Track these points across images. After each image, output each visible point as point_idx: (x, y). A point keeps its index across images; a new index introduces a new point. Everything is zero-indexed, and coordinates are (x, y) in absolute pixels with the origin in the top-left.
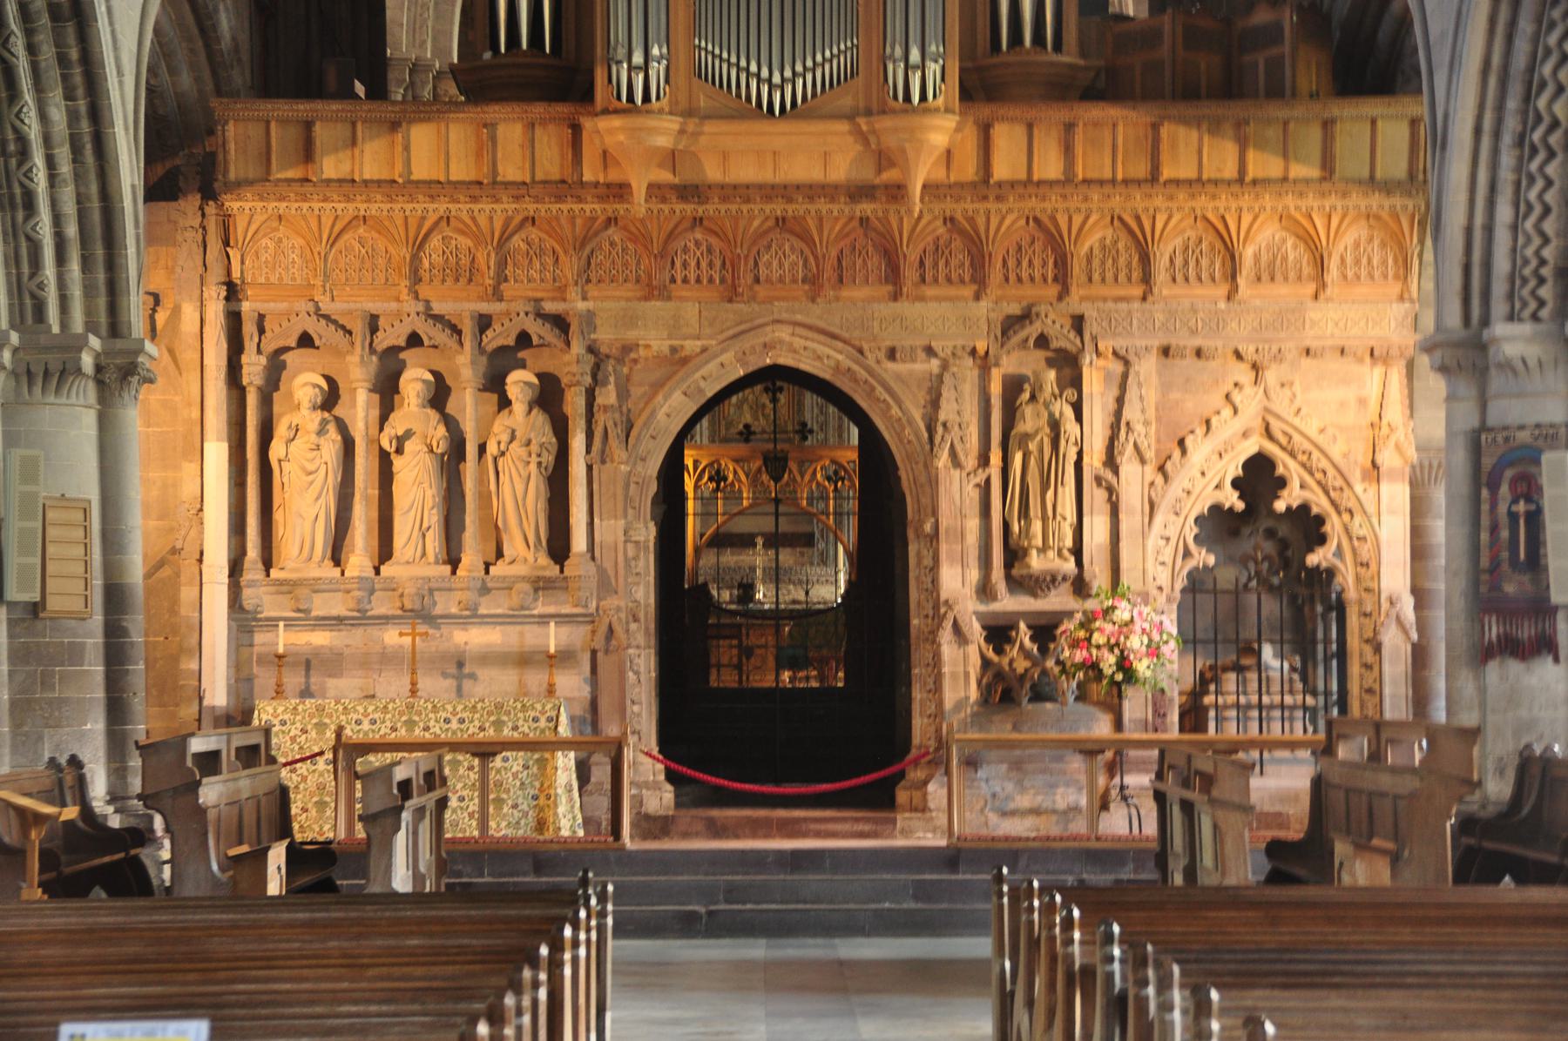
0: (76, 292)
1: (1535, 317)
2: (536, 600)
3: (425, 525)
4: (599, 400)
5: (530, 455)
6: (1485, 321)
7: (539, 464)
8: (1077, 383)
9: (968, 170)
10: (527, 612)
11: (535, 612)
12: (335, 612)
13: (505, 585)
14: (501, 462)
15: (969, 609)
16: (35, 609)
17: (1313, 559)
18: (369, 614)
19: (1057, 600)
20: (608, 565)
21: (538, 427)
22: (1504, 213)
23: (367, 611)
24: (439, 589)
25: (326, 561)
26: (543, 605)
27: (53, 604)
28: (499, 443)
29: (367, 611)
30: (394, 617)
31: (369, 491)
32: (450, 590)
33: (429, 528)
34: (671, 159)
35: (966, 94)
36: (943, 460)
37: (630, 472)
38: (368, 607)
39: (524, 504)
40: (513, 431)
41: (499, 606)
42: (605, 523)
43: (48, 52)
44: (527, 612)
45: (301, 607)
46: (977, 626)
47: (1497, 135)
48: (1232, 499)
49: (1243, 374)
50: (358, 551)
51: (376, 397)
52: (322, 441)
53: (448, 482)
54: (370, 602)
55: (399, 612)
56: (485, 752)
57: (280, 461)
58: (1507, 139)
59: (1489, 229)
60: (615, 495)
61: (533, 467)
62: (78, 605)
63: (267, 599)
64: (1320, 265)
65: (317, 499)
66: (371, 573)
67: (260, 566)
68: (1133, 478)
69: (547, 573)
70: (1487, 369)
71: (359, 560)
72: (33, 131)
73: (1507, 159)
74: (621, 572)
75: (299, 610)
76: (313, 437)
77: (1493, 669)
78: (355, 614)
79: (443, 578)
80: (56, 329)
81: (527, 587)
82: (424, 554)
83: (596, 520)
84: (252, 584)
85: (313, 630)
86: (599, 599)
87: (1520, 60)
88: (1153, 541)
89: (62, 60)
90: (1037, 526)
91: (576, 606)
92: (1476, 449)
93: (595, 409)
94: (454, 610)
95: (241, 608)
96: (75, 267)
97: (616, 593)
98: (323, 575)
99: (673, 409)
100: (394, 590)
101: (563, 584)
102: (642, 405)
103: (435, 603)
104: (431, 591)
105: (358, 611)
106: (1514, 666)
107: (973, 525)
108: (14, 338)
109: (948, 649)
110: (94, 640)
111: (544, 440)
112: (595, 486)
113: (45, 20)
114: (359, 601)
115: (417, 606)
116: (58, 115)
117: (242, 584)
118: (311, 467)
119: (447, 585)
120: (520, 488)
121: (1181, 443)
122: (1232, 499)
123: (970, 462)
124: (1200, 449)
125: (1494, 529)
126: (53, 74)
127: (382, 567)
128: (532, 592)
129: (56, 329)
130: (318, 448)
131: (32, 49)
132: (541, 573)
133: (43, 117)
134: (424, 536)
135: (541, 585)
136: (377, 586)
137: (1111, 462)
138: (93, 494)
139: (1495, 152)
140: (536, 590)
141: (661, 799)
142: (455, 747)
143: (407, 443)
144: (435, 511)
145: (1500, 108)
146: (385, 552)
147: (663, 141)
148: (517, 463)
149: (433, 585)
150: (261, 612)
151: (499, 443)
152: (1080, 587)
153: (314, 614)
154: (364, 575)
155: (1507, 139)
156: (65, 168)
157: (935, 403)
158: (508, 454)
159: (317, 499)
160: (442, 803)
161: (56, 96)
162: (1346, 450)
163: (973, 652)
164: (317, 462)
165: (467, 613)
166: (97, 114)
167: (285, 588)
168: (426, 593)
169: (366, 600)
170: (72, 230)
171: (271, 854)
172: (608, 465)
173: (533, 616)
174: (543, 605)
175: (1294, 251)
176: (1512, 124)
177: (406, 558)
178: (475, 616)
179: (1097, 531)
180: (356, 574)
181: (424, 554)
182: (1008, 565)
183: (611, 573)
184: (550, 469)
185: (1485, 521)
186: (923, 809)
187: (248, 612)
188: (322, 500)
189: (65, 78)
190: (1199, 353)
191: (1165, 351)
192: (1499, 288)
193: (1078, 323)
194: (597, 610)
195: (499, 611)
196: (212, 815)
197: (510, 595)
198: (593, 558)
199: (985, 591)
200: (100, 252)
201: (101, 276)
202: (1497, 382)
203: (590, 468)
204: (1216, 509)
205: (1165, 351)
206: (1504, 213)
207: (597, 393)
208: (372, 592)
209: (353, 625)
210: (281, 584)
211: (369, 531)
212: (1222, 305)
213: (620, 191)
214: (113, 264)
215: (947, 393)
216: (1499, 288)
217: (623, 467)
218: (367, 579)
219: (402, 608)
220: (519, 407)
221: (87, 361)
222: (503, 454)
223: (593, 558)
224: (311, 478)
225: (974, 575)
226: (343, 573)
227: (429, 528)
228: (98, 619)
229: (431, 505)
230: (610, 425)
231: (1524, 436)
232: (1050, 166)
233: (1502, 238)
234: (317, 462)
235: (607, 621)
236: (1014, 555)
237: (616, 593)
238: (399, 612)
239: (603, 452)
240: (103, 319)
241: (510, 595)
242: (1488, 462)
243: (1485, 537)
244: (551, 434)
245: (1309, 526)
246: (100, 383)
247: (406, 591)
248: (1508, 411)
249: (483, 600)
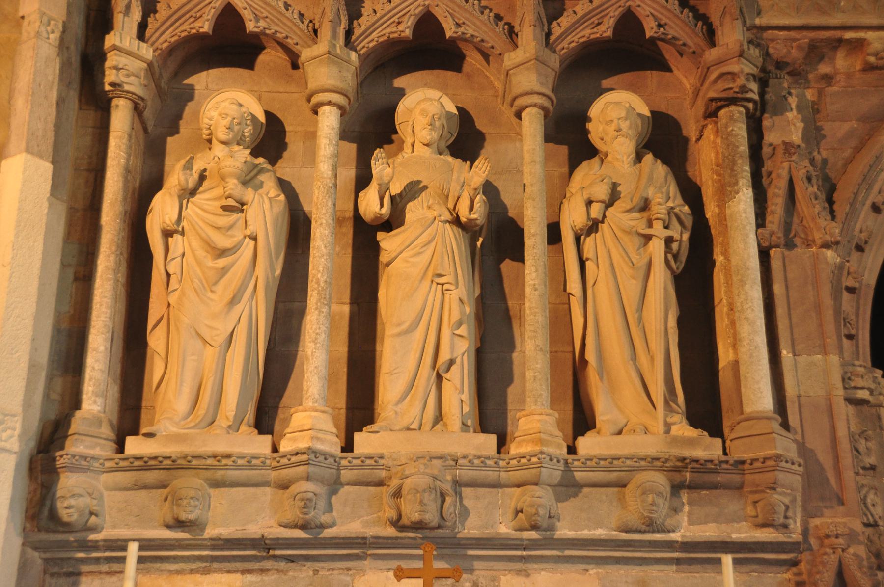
2: (676, 510)
3: (444, 356)
4: (771, 137)
5: (650, 226)
7: (669, 241)
10: (658, 537)
11: (675, 536)
12: (254, 530)
13: (613, 476)
14: (588, 244)
18: (327, 533)
20: (818, 444)
23: (322, 527)
24: (473, 484)
25: (244, 428)
26: (691, 523)
28: (589, 203)
29: (322, 527)
30: (379, 542)
31: (334, 307)
32: (496, 485)
33: (451, 362)
37: (841, 267)
38: (325, 518)
39: (640, 320)
40: (615, 185)
41: (599, 525)
42: (803, 359)
44: (658, 537)
45: (183, 516)
50: (308, 403)
51: (351, 148)
52: (249, 195)
53: (482, 287)
54: (330, 508)
55: (391, 532)
57: (167, 234)
60: (818, 307)
61: (657, 248)
63: (112, 501)
65: (234, 301)
66: (332, 444)
67: (107, 431)
69: (699, 453)
74: (847, 459)
75: (179, 524)
76: (233, 185)
78: (298, 534)
79: (483, 459)
81: (660, 480)
82: (439, 417)
83: (785, 354)
84: (83, 465)
85: (206, 572)
86: (808, 515)
91: (764, 525)
93: (766, 151)
94: (505, 529)
95: (54, 516)
97: (841, 502)
98: (236, 449)
100: (380, 484)
101: (736, 478)
102: (848, 153)
103: (465, 513)
104: (458, 484)
105: (304, 527)
111: (670, 204)
112: (778, 289)
114: (307, 504)
115: (431, 517)
117: (60, 463)
118: (223, 242)
119: (491, 475)
120: (631, 288)
127: (357, 436)
128: (667, 489)
130: (240, 207)
132: (687, 453)
134: (439, 378)
136: (346, 475)
140: (676, 488)
143: (410, 206)
144: (462, 330)
148: (625, 239)
149: (465, 474)
150: (94, 529)
151: (589, 203)
153: (211, 532)
154: (319, 446)
158: (604, 227)
159: (234, 301)
164: (238, 234)
165: (533, 535)
167: (151, 476)
168: (448, 487)
169: (322, 504)
172: (798, 251)
173: (670, 545)
174: (691, 523)
177: (405, 422)
178: (550, 542)
180: (302, 445)
181: (439, 417)
183: (825, 458)
184: (683, 257)
187: (67, 527)
188: (242, 307)
194: (805, 532)
195: (600, 533)
197: (622, 500)
198: (785, 425)
203: (764, 255)
207: (766, 123)
208: (335, 485)
209: (290, 559)
210: (146, 468)
211: (330, 379)
217: (829, 254)
218: (326, 455)
219: (397, 523)
222: (593, 227)
223: (785, 425)
224: (222, 262)
226: (275, 449)
227: (451, 362)
229: (456, 316)
230: (800, 175)
234: (238, 234)
235: (833, 559)
237: (841, 502)
238: (391, 532)
239: (787, 226)
241: (622, 500)
244: (679, 200)
247: (408, 483)
249: (566, 509)
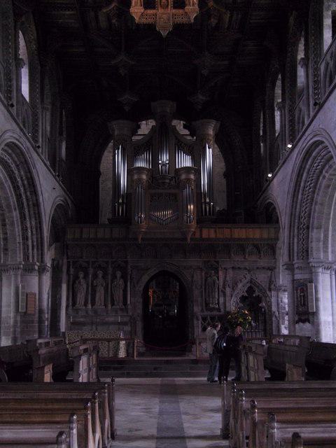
0: (36, 255)
1: (302, 259)
6: (294, 260)
8: (218, 273)
9: (197, 235)
15: (199, 315)
16: (25, 313)
17: (260, 305)
19: (215, 313)
21: (121, 282)
22: (296, 240)
27: (29, 312)
34: (146, 233)
35: (197, 223)
36: (194, 287)
43: (32, 212)
46: (200, 317)
47: (294, 227)
48: (246, 294)
49: (246, 272)
56: (109, 341)
58: (296, 227)
59: (293, 243)
62: (33, 313)
64: (259, 253)
68: (228, 290)
70: (294, 269)
71: (90, 306)
72: (28, 225)
73: (296, 231)
77: (297, 326)
80: (31, 261)
87: (297, 214)
88: (232, 302)
89: (35, 213)
90: (211, 299)
92: (293, 283)
96: (35, 250)
99: (145, 278)
106: (301, 324)
107: (199, 299)
108: (23, 263)
109: (195, 322)
110: (36, 318)
113: (32, 206)
116: (33, 223)
121: (236, 284)
122: (246, 294)
123: (199, 287)
124: (240, 286)
125: (297, 298)
126: (33, 216)
129: (31, 261)
131: (29, 211)
133: (31, 223)
135: (122, 310)
137: (225, 288)
138: (37, 293)
139: (294, 230)
141: (142, 350)
142: (102, 340)
145: (294, 222)
146: (93, 304)
147: (143, 230)
152: (219, 310)
155: (296, 227)
156: (34, 233)
157: (193, 277)
160: (98, 352)
161: (33, 219)
162: (265, 285)
163: (200, 322)
166: (40, 223)
170: (35, 244)
171: (46, 367)
175: (255, 250)
176: (296, 224)
179: (222, 300)
182: (206, 306)
185: (295, 297)
186: (190, 351)
189: (35, 217)
190: (239, 268)
191: (233, 268)
192: (295, 254)
193: (217, 262)
196: (42, 356)
199: (202, 311)
200: (40, 247)
201: (40, 252)
202: (296, 271)
204: (243, 296)
205: (233, 268)
206: (296, 240)
212: (243, 260)
213: (136, 239)
214: (42, 250)
215: (195, 275)
216: (295, 254)
220: (118, 278)
221: (36, 268)
225: (200, 308)
228: (37, 315)
231: (302, 281)
232: (213, 235)
233: (295, 244)
236: (207, 304)
240: (40, 260)
242: (295, 286)
243: (296, 300)
245: (259, 299)
246: (39, 272)
248: (297, 277)
